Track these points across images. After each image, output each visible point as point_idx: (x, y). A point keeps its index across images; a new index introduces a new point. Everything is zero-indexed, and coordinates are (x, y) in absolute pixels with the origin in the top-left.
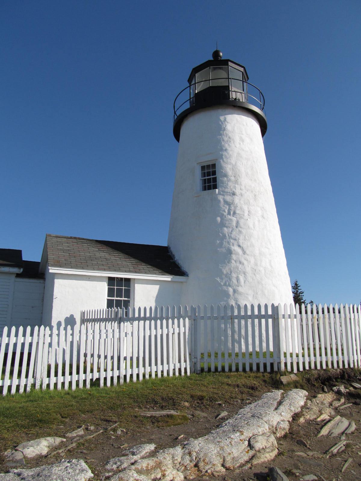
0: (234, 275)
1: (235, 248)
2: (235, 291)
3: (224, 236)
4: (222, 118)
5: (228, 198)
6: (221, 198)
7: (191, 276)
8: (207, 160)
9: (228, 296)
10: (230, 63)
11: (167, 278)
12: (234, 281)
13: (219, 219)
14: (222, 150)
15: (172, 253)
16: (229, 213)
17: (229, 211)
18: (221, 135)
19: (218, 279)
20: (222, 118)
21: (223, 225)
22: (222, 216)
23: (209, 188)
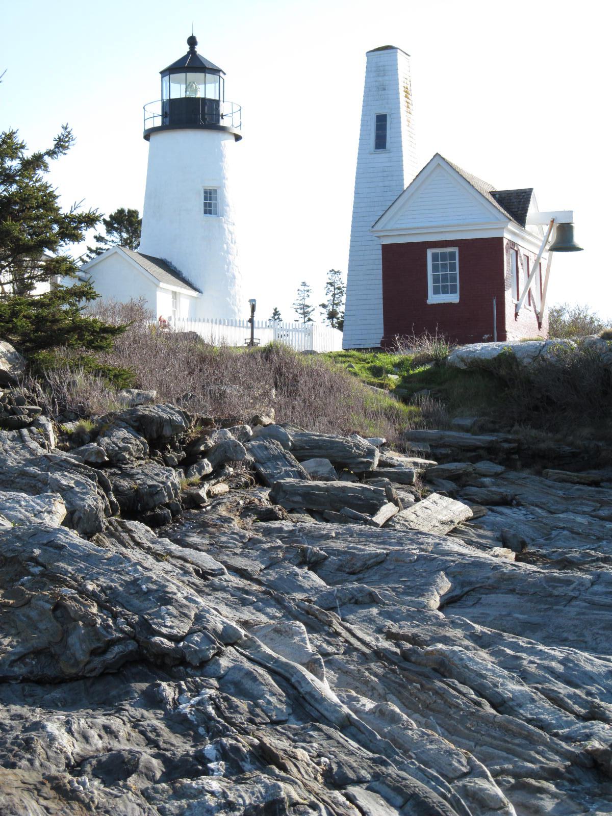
0: (237, 297)
1: (236, 274)
2: (239, 310)
3: (230, 262)
4: (222, 143)
5: (231, 228)
6: (225, 226)
7: (205, 294)
8: (210, 185)
9: (235, 313)
10: (221, 74)
11: (195, 294)
12: (238, 300)
13: (225, 246)
14: (224, 178)
15: (175, 268)
16: (232, 242)
17: (232, 239)
18: (222, 162)
19: (228, 299)
20: (222, 143)
21: (228, 252)
22: (227, 244)
23: (210, 213)
